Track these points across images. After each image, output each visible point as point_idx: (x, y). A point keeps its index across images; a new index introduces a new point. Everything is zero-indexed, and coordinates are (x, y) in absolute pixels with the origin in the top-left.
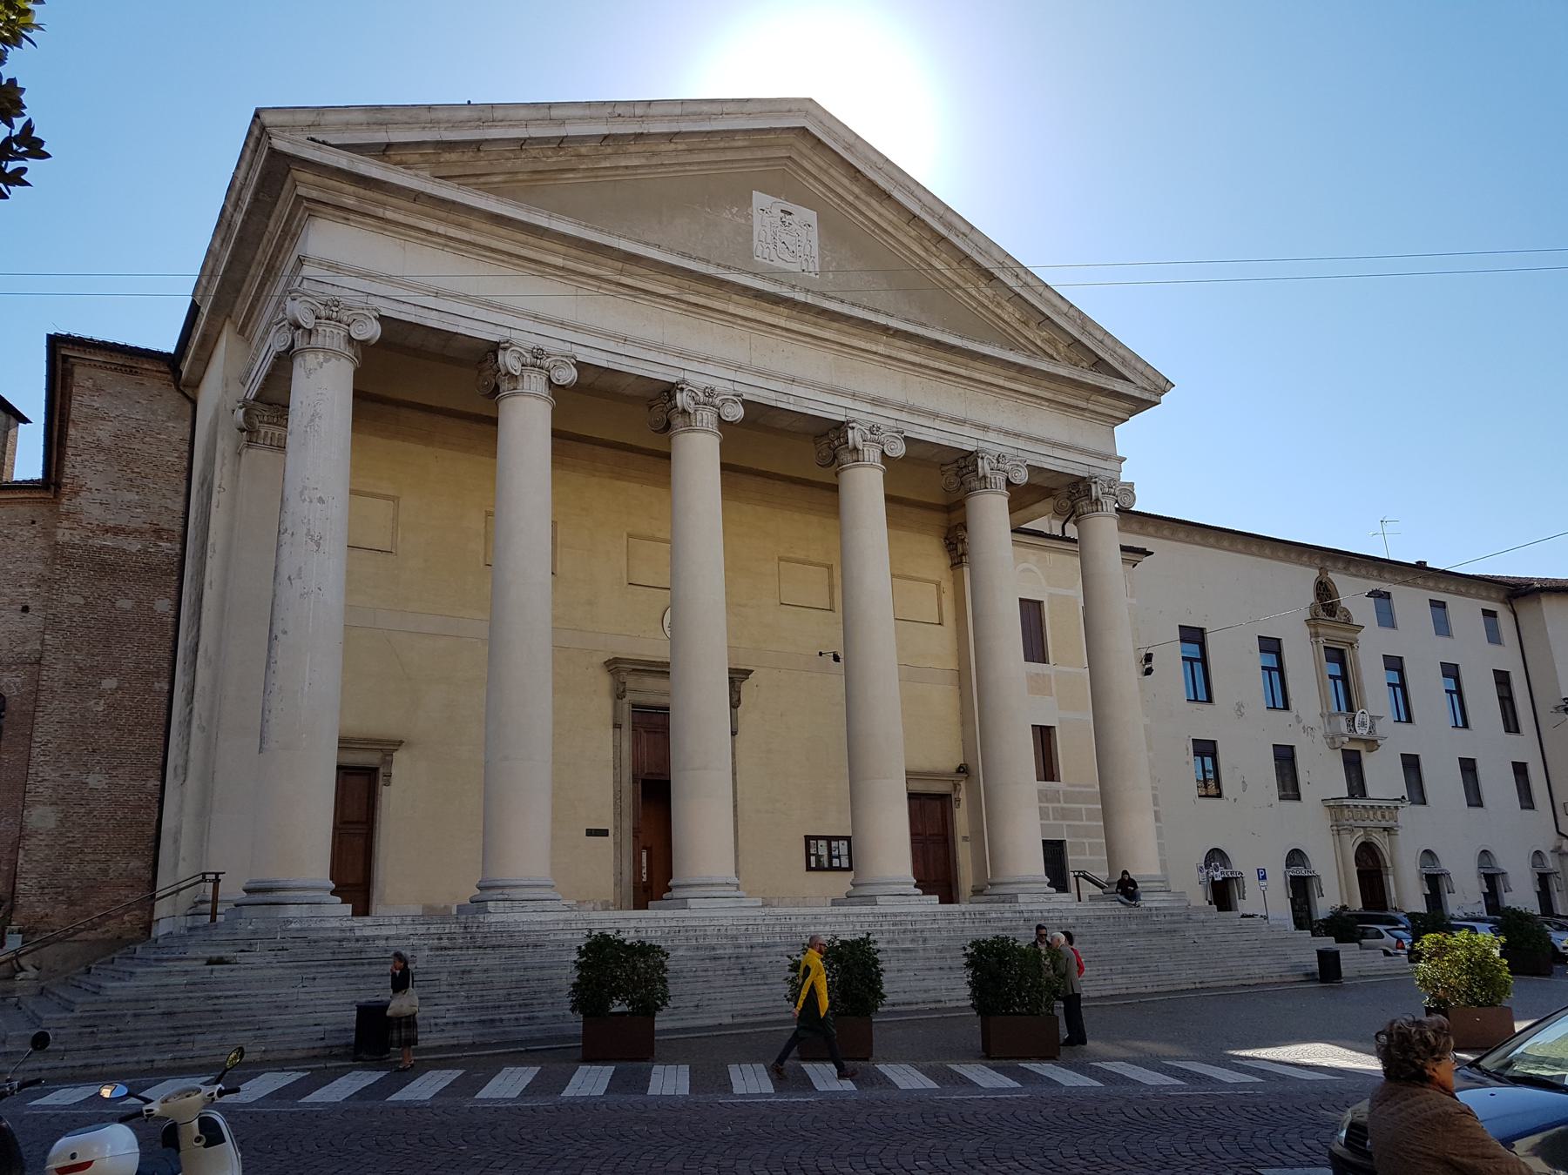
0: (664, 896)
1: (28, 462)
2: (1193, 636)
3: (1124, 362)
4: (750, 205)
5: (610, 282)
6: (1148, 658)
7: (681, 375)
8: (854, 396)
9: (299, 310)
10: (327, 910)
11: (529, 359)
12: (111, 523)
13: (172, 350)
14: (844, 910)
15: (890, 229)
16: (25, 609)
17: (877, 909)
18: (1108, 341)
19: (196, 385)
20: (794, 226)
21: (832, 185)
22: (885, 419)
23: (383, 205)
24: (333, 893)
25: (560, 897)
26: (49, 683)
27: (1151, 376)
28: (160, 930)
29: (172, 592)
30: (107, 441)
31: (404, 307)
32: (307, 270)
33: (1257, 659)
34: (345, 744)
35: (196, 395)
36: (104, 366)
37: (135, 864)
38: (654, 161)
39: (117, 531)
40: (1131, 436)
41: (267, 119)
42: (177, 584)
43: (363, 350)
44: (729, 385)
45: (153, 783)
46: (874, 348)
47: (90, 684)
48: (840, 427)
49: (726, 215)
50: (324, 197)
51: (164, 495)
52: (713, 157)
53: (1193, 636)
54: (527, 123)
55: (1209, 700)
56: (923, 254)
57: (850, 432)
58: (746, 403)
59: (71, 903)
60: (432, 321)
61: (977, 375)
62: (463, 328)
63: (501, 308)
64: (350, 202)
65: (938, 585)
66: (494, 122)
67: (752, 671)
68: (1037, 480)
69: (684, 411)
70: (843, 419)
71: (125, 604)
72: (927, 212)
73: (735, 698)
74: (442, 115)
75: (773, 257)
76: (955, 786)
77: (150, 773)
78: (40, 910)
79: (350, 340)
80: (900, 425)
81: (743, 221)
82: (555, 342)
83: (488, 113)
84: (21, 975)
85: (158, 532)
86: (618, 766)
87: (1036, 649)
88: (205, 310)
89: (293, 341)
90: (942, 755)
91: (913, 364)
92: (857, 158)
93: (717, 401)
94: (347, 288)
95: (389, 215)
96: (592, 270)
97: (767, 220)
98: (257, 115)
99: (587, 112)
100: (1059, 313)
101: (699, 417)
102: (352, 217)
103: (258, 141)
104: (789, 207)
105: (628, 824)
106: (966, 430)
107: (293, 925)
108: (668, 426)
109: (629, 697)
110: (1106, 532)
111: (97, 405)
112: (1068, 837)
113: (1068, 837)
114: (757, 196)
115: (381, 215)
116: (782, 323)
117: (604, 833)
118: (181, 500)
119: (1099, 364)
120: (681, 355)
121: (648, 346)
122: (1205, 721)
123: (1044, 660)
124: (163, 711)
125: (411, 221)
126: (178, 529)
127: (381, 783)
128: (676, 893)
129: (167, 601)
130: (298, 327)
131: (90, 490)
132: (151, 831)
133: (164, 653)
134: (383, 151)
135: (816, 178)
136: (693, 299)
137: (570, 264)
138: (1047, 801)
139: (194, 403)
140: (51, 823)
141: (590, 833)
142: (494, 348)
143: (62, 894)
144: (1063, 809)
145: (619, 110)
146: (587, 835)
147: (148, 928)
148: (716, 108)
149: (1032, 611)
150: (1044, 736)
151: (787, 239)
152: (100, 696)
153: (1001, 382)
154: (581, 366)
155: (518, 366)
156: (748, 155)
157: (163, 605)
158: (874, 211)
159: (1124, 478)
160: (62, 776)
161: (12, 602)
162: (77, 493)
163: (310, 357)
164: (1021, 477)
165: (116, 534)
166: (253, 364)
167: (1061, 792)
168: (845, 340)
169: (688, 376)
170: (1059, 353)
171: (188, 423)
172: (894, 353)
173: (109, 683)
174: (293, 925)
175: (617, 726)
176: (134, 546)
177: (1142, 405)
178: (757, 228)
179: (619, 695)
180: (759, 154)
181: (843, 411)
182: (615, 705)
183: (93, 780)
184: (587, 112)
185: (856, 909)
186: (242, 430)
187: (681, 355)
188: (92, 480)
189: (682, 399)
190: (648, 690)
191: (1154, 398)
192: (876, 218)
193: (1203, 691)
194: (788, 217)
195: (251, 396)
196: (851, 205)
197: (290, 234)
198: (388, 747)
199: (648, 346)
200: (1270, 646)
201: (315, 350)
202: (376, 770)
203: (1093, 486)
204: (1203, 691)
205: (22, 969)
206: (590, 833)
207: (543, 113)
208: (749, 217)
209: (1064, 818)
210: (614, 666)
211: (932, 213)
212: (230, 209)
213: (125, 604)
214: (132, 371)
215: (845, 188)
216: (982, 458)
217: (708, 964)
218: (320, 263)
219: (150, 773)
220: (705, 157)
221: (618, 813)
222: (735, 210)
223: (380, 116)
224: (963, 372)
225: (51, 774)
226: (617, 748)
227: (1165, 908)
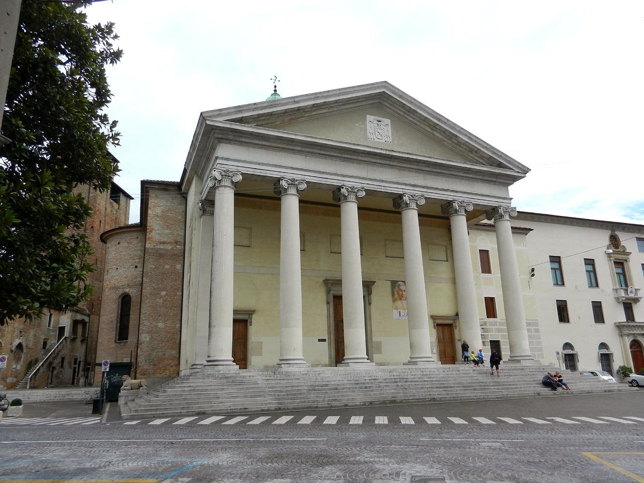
0: (343, 362)
1: (134, 217)
2: (556, 260)
3: (510, 162)
4: (366, 120)
5: (317, 153)
6: (533, 270)
7: (343, 182)
8: (406, 185)
9: (216, 174)
10: (231, 367)
11: (290, 182)
12: (162, 241)
13: (179, 181)
14: (405, 367)
15: (417, 123)
16: (136, 267)
17: (417, 367)
18: (503, 156)
19: (187, 193)
20: (382, 126)
21: (396, 110)
22: (417, 192)
24: (234, 362)
25: (305, 362)
26: (145, 294)
27: (522, 168)
28: (182, 374)
29: (182, 262)
30: (160, 214)
31: (249, 169)
32: (219, 161)
33: (583, 268)
34: (236, 312)
35: (187, 197)
36: (158, 189)
37: (174, 352)
38: (332, 110)
39: (164, 243)
40: (514, 190)
41: (204, 115)
42: (182, 260)
43: (235, 185)
44: (360, 185)
45: (178, 326)
46: (412, 167)
47: (158, 293)
48: (401, 196)
49: (357, 125)
50: (223, 137)
51: (178, 230)
52: (352, 106)
53: (556, 260)
54: (286, 104)
55: (563, 284)
56: (430, 131)
57: (404, 197)
58: (366, 190)
59: (155, 365)
60: (258, 173)
62: (269, 174)
63: (280, 166)
64: (231, 137)
65: (446, 247)
66: (276, 106)
67: (375, 282)
68: (478, 208)
69: (344, 195)
70: (402, 193)
71: (167, 267)
72: (431, 116)
73: (370, 291)
74: (258, 106)
75: (375, 138)
76: (454, 322)
77: (177, 322)
78: (146, 367)
79: (232, 182)
80: (423, 193)
81: (363, 126)
82: (298, 176)
84: (141, 388)
85: (176, 243)
86: (328, 317)
87: (486, 268)
88: (188, 171)
89: (215, 183)
90: (445, 309)
91: (427, 171)
92: (404, 100)
93: (356, 190)
94: (232, 166)
95: (244, 140)
96: (310, 150)
97: (372, 125)
98: (201, 114)
99: (307, 97)
100: (483, 147)
101: (349, 197)
102: (232, 142)
103: (202, 121)
104: (380, 119)
105: (333, 337)
106: (449, 193)
107: (221, 372)
108: (339, 200)
109: (332, 292)
110: (506, 226)
111: (156, 202)
112: (488, 339)
113: (501, 339)
114: (370, 118)
115: (241, 140)
116: (378, 161)
117: (324, 340)
118: (183, 231)
119: (500, 165)
120: (343, 176)
121: (332, 174)
122: (561, 294)
123: (490, 272)
124: (180, 300)
125: (250, 141)
126: (182, 241)
127: (249, 324)
128: (346, 361)
129: (180, 265)
130: (216, 179)
131: (155, 230)
132: (178, 342)
133: (180, 282)
134: (241, 121)
135: (389, 108)
136: (346, 156)
137: (304, 149)
138: (494, 326)
139: (186, 199)
140: (148, 339)
141: (319, 340)
142: (279, 180)
143: (152, 362)
145: (318, 95)
146: (319, 341)
147: (178, 374)
148: (351, 90)
149: (484, 254)
150: (490, 303)
151: (379, 130)
152: (161, 297)
153: (462, 175)
154: (308, 183)
155: (286, 185)
156: (364, 103)
157: (179, 267)
158: (411, 117)
159: (512, 205)
160: (151, 324)
161: (132, 265)
162: (151, 231)
163: (220, 189)
164: (470, 208)
165: (164, 244)
166: (203, 188)
168: (402, 165)
169: (345, 183)
170: (485, 161)
171: (184, 206)
172: (420, 168)
173: (163, 293)
174: (221, 372)
175: (328, 303)
176: (169, 247)
177: (515, 179)
178: (368, 128)
179: (328, 292)
180: (368, 102)
181: (402, 190)
182: (327, 295)
183: (160, 325)
184: (307, 97)
185: (410, 367)
186: (201, 210)
187: (343, 176)
188: (156, 227)
189: (343, 191)
190: (334, 292)
191: (523, 175)
192: (412, 120)
193: (560, 281)
194: (380, 123)
195: (203, 198)
196: (403, 116)
197: (214, 149)
198: (251, 313)
199: (332, 174)
200: (590, 262)
201: (222, 186)
202: (247, 320)
203: (500, 210)
204: (560, 281)
205: (142, 386)
206: (319, 340)
207: (293, 100)
208: (365, 125)
209: (499, 332)
210: (326, 282)
211: (433, 117)
212: (194, 141)
213: (167, 267)
214: (167, 190)
215: (400, 110)
216: (455, 203)
217: (354, 386)
218: (222, 158)
219: (177, 322)
221: (329, 333)
222: (360, 123)
223: (239, 109)
224: (446, 172)
225: (146, 323)
226: (328, 310)
227: (530, 366)
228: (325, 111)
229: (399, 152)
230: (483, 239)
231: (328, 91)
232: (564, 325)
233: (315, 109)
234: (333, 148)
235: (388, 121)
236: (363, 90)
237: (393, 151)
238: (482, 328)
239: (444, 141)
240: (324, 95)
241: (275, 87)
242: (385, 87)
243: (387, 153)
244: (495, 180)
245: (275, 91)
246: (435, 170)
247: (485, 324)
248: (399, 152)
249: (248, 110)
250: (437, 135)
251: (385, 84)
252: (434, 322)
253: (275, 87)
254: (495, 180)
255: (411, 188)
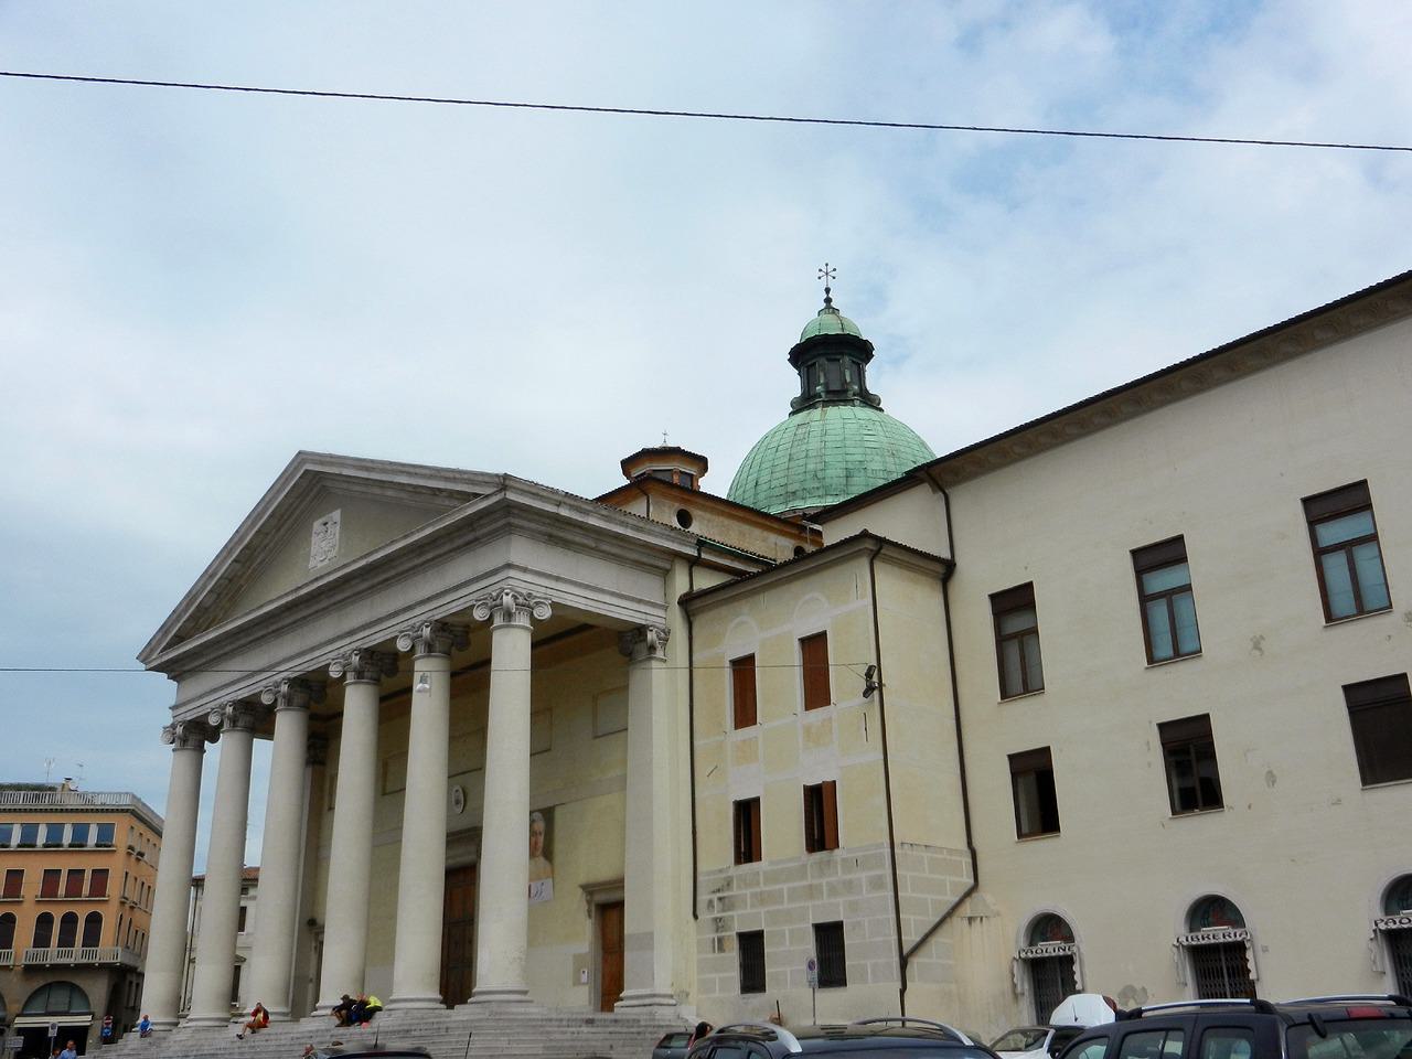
23: (184, 665)
54: (205, 586)
61: (401, 569)
83: (190, 597)
114: (317, 525)
134: (179, 639)
144: (761, 893)
145: (230, 546)
167: (761, 873)
168: (333, 600)
180: (308, 499)
220: (286, 526)
223: (164, 630)
224: (393, 572)
228: (261, 557)
229: (354, 561)
230: (743, 623)
231: (237, 531)
232: (1202, 824)
233: (248, 564)
234: (257, 624)
235: (336, 515)
236: (279, 492)
237: (300, 588)
238: (720, 899)
239: (402, 499)
240: (236, 539)
241: (828, 290)
242: (304, 461)
243: (290, 598)
244: (470, 537)
245: (828, 301)
246: (376, 580)
247: (728, 885)
248: (306, 585)
249: (172, 625)
250: (390, 493)
251: (302, 457)
252: (589, 902)
253: (828, 290)
254: (470, 537)
255: (348, 640)
